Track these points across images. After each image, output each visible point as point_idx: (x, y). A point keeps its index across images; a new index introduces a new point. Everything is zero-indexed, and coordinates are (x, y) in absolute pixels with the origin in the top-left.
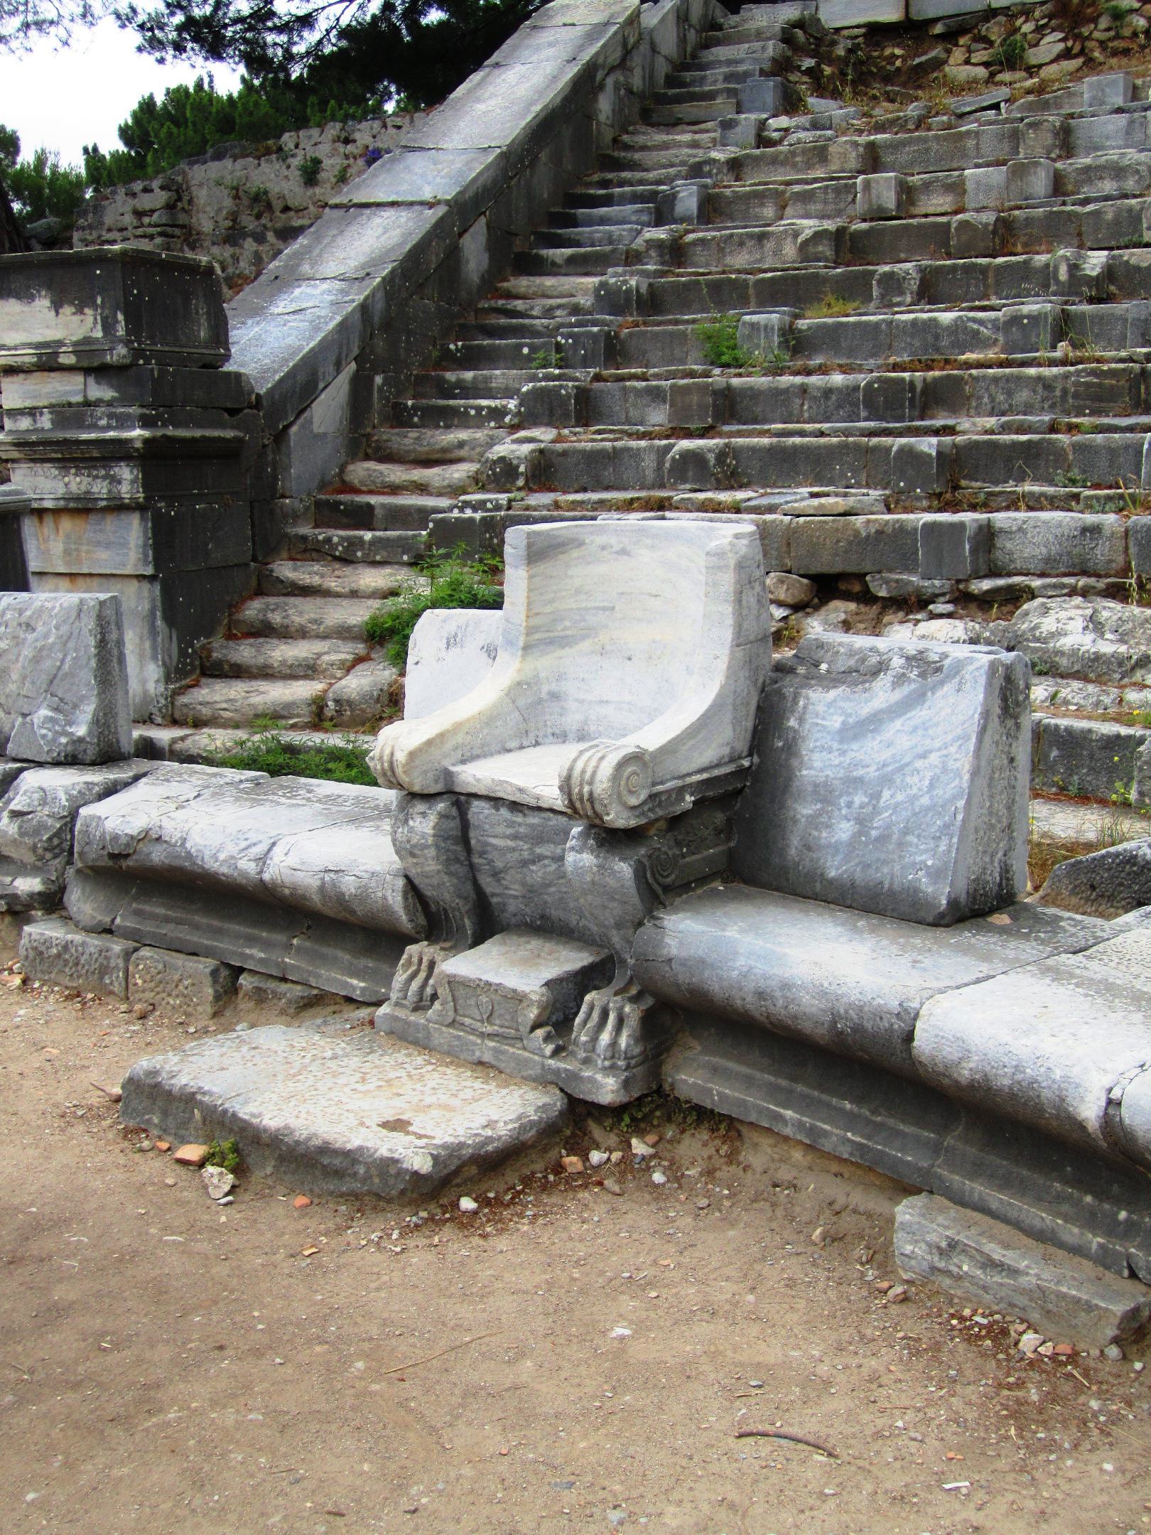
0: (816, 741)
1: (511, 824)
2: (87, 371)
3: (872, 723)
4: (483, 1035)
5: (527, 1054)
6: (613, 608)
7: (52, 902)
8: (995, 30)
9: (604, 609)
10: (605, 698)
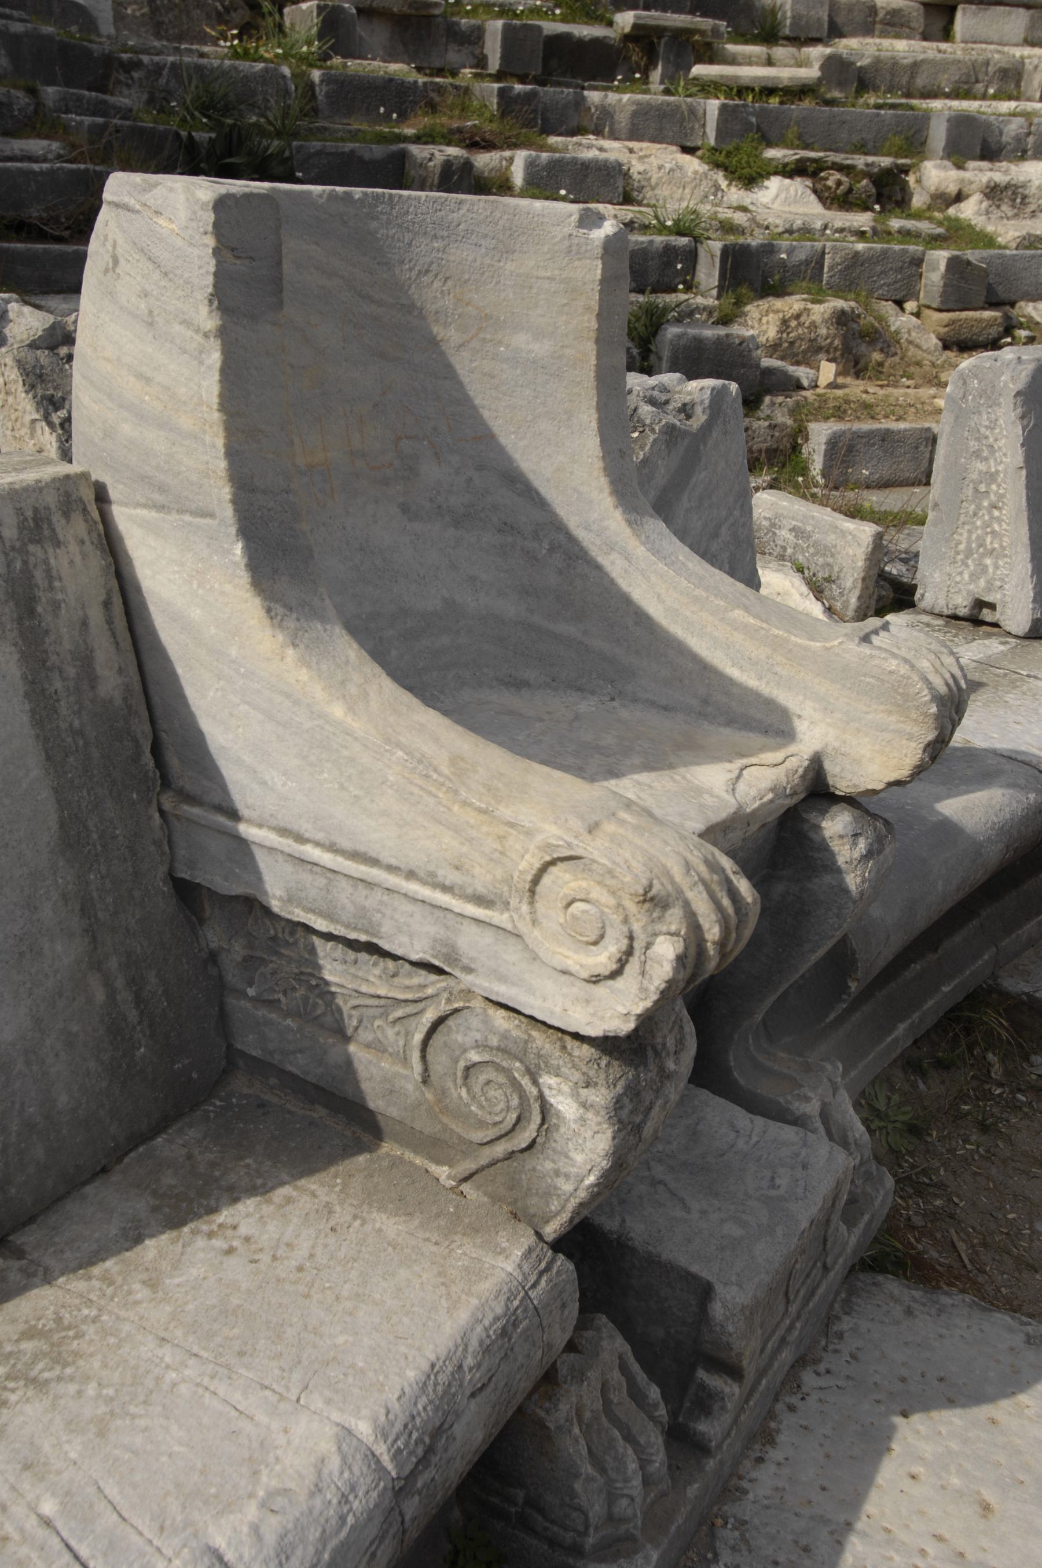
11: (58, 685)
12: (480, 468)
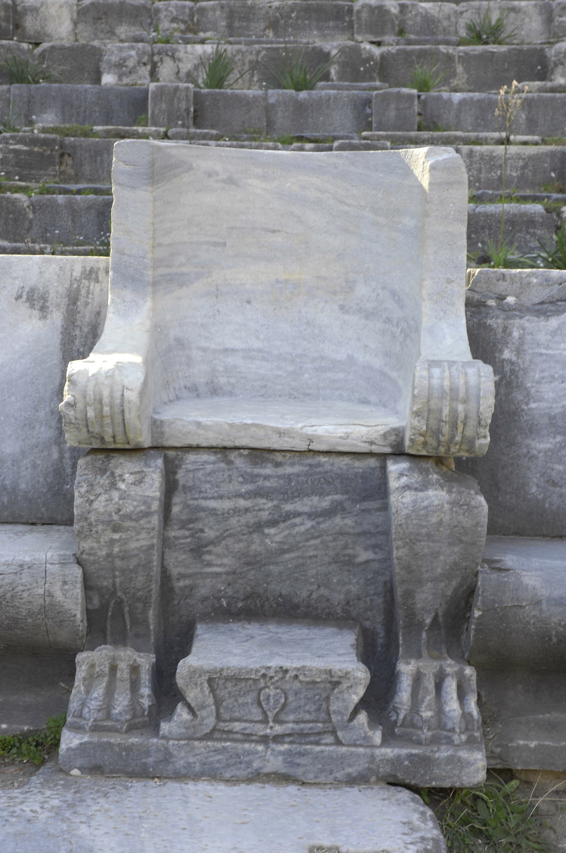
0: (542, 371)
1: (251, 478)
4: (264, 740)
5: (344, 749)
6: (224, 244)
9: (215, 244)
10: (228, 346)
11: (78, 332)
12: (383, 288)
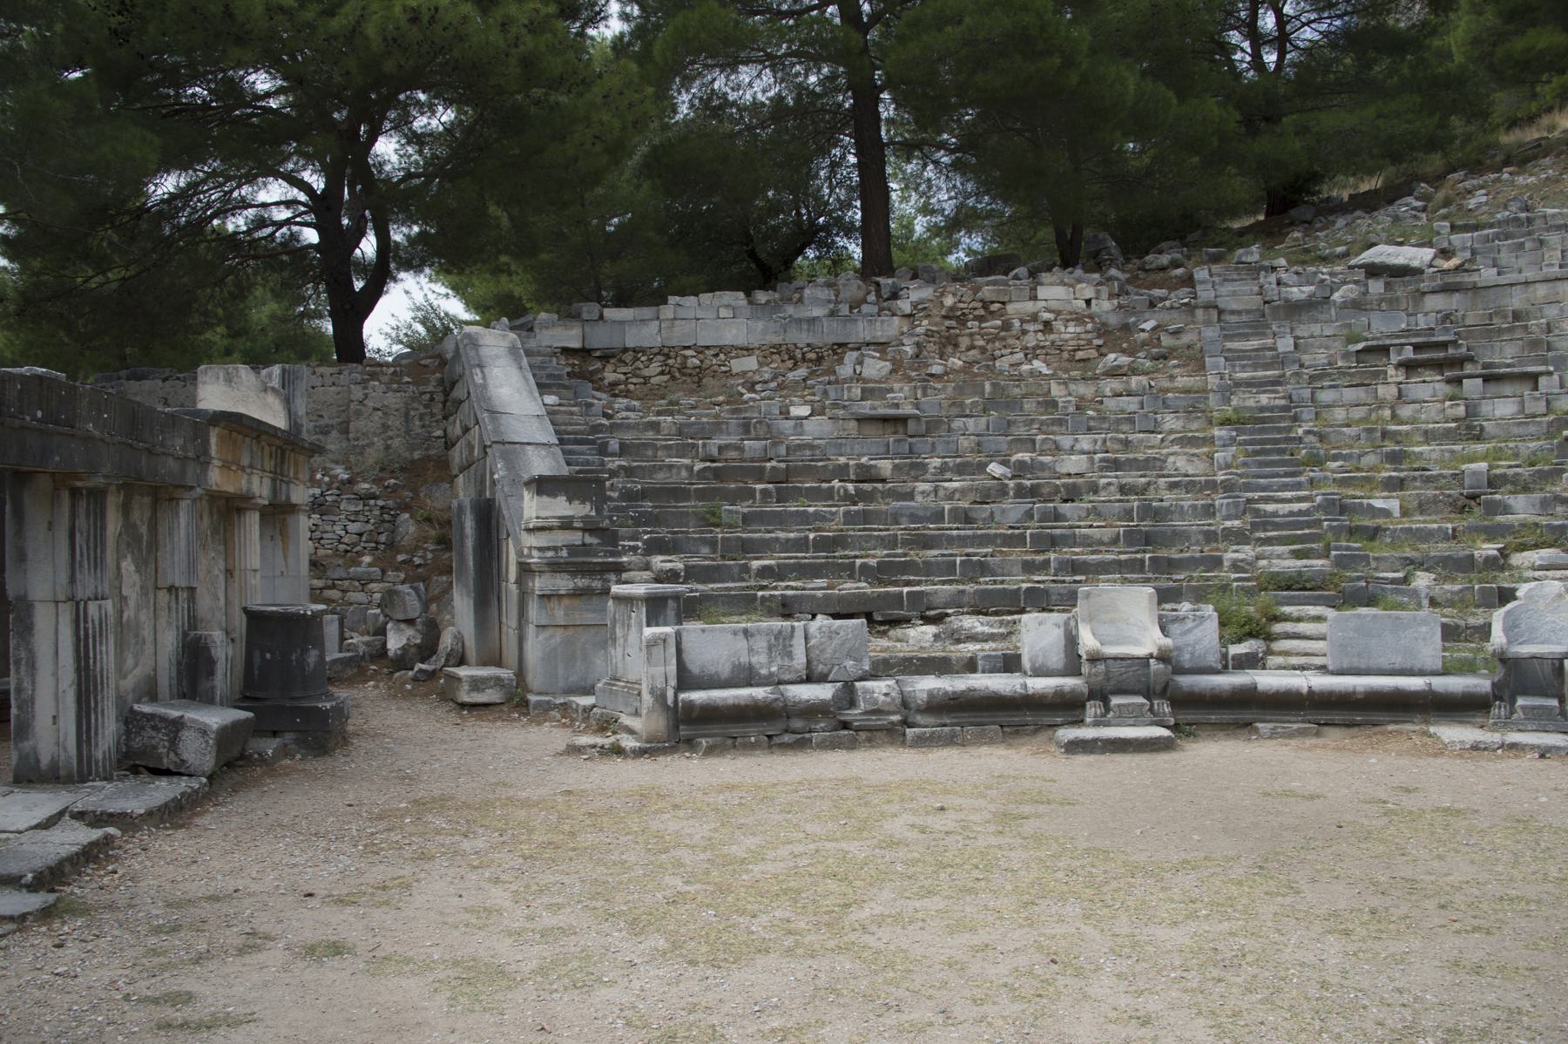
2: (584, 530)
3: (1190, 631)
7: (906, 723)
8: (628, 357)
